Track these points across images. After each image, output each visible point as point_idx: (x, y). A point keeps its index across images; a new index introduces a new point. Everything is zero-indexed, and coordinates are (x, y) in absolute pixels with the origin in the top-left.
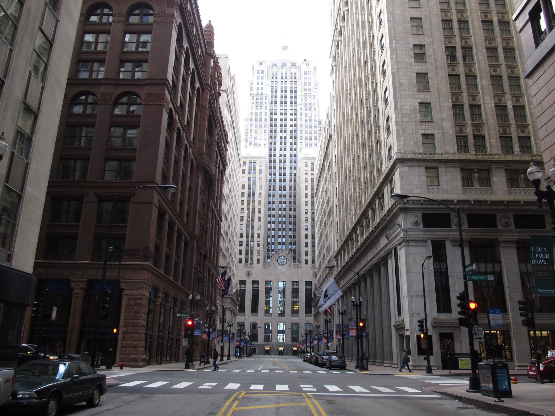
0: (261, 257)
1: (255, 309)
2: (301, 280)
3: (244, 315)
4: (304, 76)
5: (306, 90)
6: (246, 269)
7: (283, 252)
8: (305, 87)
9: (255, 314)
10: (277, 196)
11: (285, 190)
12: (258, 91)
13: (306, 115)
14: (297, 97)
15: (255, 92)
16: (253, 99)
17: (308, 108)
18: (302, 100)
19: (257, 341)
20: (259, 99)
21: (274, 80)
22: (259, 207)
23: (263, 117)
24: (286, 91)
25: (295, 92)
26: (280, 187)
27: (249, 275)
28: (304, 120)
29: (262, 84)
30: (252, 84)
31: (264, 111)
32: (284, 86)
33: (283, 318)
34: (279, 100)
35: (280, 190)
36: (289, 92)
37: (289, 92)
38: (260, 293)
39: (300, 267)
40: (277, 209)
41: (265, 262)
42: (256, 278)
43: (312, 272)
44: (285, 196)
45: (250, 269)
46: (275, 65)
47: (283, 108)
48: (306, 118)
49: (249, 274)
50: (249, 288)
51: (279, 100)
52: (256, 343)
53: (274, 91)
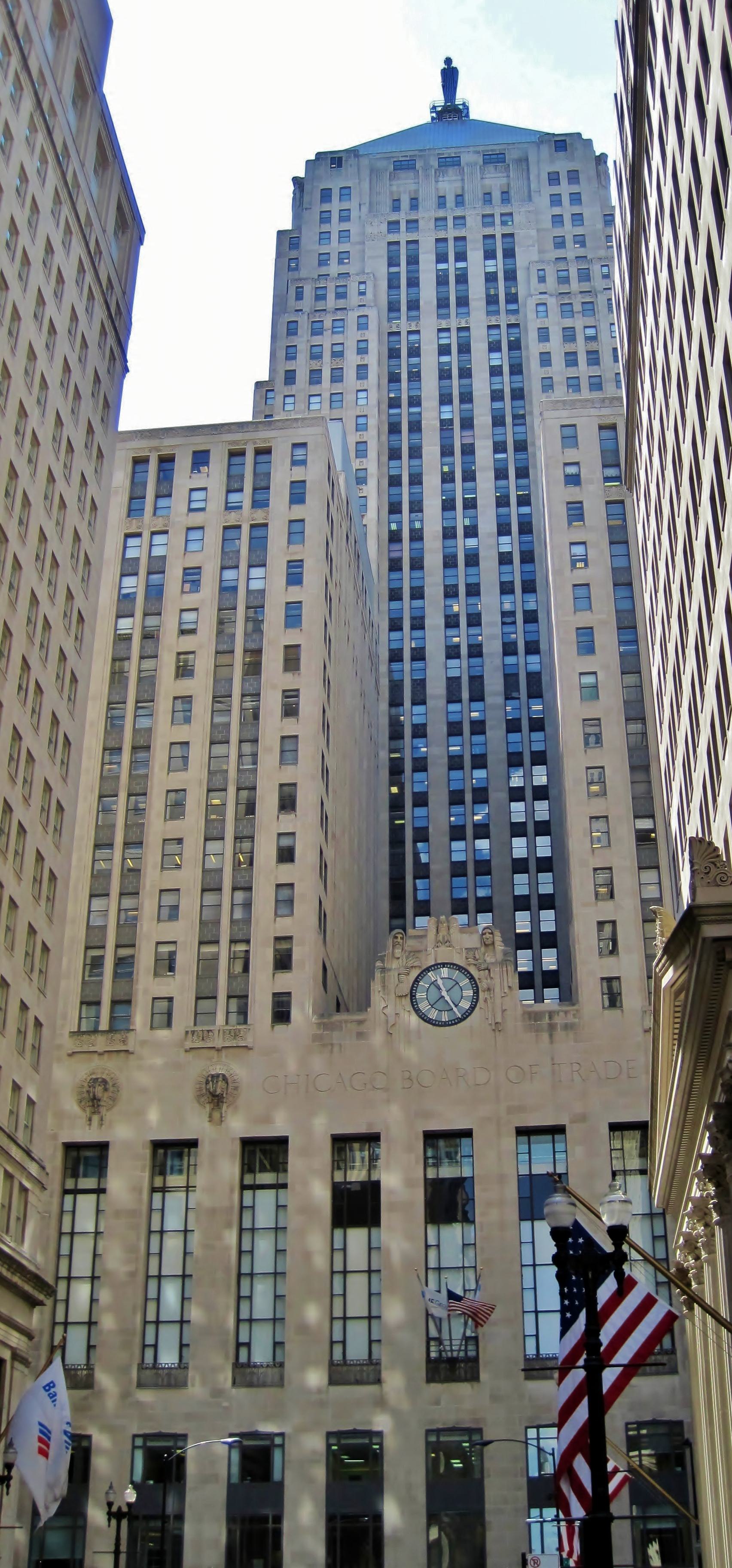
2: (582, 1118)
4: (548, 190)
5: (560, 243)
7: (447, 942)
8: (558, 232)
10: (437, 729)
11: (477, 695)
12: (323, 270)
13: (569, 335)
14: (520, 275)
16: (299, 296)
17: (577, 307)
18: (542, 279)
20: (331, 296)
21: (402, 217)
22: (289, 681)
23: (352, 360)
24: (461, 256)
25: (509, 254)
26: (453, 683)
28: (558, 360)
32: (451, 233)
33: (464, 1389)
34: (428, 293)
35: (453, 697)
36: (475, 255)
37: (475, 255)
39: (567, 1027)
40: (438, 798)
44: (478, 727)
47: (453, 323)
48: (570, 347)
51: (428, 293)
53: (402, 261)
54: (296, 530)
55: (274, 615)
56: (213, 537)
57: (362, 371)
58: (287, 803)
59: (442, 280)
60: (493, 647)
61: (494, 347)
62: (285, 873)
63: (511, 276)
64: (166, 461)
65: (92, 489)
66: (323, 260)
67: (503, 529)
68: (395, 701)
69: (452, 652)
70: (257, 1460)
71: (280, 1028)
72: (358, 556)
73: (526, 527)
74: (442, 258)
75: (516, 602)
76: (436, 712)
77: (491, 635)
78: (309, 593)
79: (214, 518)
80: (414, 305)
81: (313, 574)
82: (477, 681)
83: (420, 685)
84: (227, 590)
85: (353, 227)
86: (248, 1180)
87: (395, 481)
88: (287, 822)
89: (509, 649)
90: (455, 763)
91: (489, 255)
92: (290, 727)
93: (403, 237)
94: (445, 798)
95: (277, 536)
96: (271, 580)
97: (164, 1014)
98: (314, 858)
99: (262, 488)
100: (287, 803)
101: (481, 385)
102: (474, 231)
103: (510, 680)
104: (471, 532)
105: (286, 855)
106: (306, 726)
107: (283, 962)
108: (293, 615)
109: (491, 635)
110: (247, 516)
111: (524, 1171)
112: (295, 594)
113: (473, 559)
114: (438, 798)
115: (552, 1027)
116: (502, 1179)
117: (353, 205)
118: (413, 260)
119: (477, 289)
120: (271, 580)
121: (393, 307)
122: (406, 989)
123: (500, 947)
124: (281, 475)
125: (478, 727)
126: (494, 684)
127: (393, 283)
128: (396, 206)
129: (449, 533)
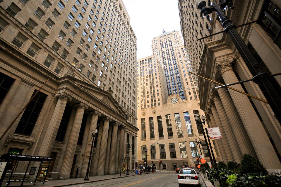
0: (161, 102)
1: (161, 135)
3: (154, 140)
6: (153, 110)
7: (174, 96)
9: (161, 138)
11: (174, 79)
15: (154, 47)
19: (166, 158)
23: (158, 53)
24: (167, 43)
25: (171, 41)
26: (171, 78)
27: (154, 113)
29: (157, 44)
30: (152, 45)
31: (158, 51)
33: (182, 138)
34: (164, 46)
35: (172, 79)
36: (168, 42)
37: (168, 42)
38: (163, 123)
41: (163, 104)
42: (159, 114)
43: (196, 104)
44: (174, 81)
45: (155, 110)
46: (161, 37)
49: (154, 112)
50: (155, 121)
51: (164, 46)
52: (165, 160)
54: (155, 64)
55: (154, 71)
56: (148, 66)
57: (160, 54)
58: (157, 86)
59: (165, 45)
60: (174, 74)
61: (171, 50)
62: (158, 92)
63: (171, 43)
64: (143, 61)
65: (134, 59)
66: (155, 46)
67: (174, 64)
68: (167, 80)
69: (171, 75)
70: (162, 147)
71: (159, 106)
72: (161, 68)
73: (176, 64)
74: (165, 43)
75: (176, 70)
76: (170, 81)
77: (174, 73)
78: (157, 69)
79: (148, 64)
80: (163, 48)
81: (157, 67)
82: (174, 77)
83: (169, 79)
84: (150, 70)
85: (157, 43)
86: (158, 120)
87: (164, 63)
88: (157, 88)
89: (176, 74)
90: (173, 85)
91: (169, 42)
92: (157, 80)
93: (161, 42)
94: (172, 87)
95: (153, 65)
96: (153, 68)
97: (148, 106)
98: (160, 91)
99: (151, 61)
100: (157, 86)
101: (170, 53)
102: (168, 40)
103: (177, 77)
104: (171, 65)
105: (158, 91)
106: (158, 80)
107: (159, 100)
108: (155, 71)
109: (174, 73)
110: (150, 63)
111: (185, 116)
112: (155, 69)
113: (172, 67)
114: (172, 88)
115: (185, 102)
116: (183, 117)
117: (157, 41)
118: (163, 44)
119: (169, 45)
120: (153, 68)
121: (162, 49)
122: (170, 101)
123: (179, 96)
124: (153, 59)
125: (174, 81)
126: (175, 77)
127: (161, 47)
128: (160, 40)
129: (169, 66)
